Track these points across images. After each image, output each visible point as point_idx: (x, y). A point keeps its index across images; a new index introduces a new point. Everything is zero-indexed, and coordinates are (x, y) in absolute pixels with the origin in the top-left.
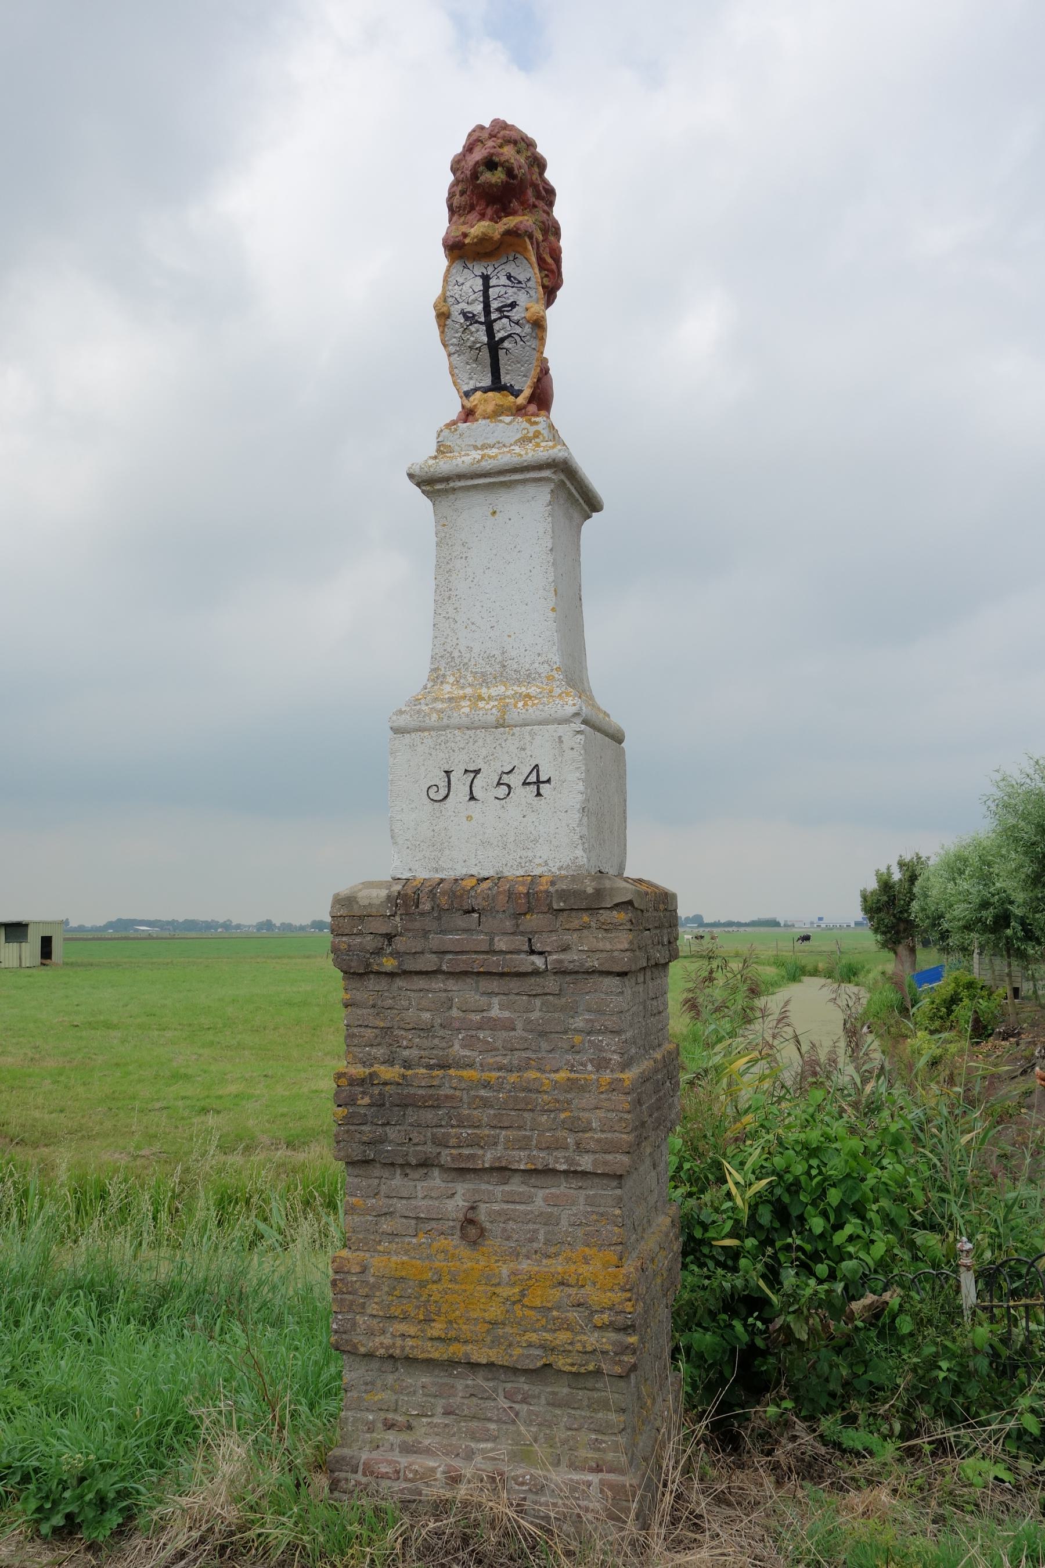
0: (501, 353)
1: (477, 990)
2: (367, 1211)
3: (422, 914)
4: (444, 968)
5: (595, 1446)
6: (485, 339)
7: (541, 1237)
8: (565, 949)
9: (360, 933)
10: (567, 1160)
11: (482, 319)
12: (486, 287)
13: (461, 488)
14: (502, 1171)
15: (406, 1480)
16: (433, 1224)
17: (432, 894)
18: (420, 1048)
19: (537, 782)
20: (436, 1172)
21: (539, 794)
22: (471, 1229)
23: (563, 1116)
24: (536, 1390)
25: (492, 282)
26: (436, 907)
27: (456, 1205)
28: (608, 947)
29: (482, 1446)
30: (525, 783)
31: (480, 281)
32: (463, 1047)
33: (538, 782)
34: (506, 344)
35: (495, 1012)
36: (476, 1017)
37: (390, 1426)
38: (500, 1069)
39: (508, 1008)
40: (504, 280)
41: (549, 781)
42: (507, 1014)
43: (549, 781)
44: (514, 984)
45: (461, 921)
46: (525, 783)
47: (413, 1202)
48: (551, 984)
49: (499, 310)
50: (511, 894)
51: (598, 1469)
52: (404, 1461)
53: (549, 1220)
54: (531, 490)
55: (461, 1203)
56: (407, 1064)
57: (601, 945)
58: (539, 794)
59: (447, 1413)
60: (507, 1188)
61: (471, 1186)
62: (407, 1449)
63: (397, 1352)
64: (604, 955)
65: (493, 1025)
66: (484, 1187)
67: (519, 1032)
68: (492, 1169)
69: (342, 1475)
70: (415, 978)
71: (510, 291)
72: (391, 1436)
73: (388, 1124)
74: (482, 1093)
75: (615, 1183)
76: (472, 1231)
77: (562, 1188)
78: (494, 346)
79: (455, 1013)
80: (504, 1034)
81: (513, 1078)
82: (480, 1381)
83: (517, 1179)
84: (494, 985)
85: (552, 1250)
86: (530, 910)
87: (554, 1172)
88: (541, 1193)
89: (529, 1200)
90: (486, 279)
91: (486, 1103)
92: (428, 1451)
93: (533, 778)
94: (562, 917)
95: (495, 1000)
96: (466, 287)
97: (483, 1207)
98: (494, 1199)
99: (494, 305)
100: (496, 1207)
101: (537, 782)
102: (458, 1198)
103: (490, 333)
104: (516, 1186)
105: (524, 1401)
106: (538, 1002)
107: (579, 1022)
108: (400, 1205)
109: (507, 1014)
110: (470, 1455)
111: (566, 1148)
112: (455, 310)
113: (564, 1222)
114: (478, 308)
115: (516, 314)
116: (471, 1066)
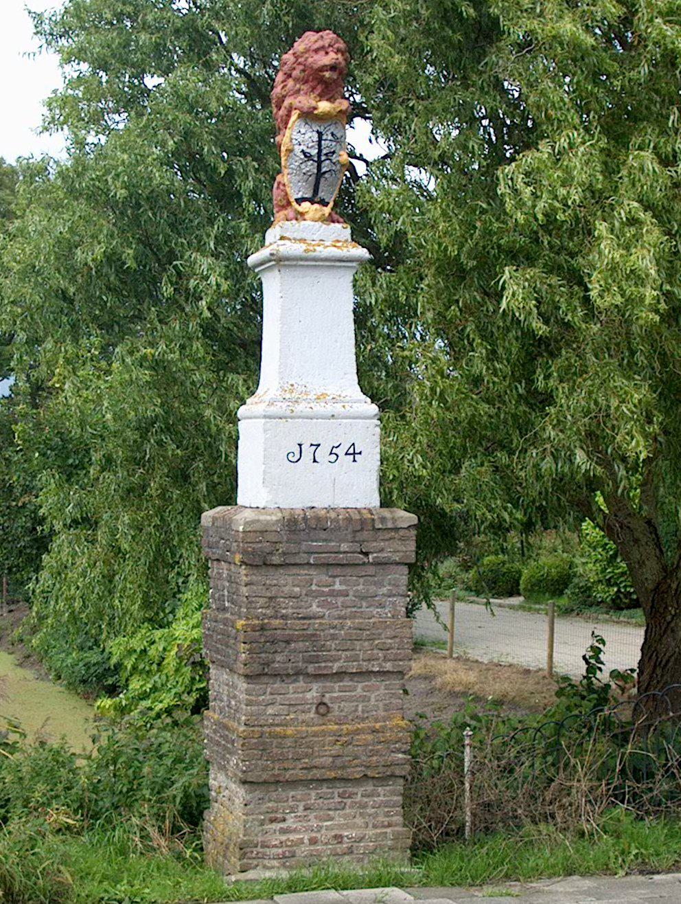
0: (322, 180)
1: (327, 575)
2: (258, 704)
3: (300, 531)
4: (312, 561)
5: (387, 815)
6: (315, 171)
7: (360, 709)
8: (382, 550)
9: (260, 542)
10: (380, 666)
11: (316, 159)
12: (320, 140)
13: (302, 266)
14: (340, 675)
15: (287, 846)
16: (300, 707)
17: (305, 519)
18: (293, 608)
19: (353, 453)
20: (301, 678)
21: (354, 461)
22: (322, 707)
23: (377, 642)
24: (355, 790)
25: (324, 137)
26: (308, 527)
27: (313, 694)
28: (404, 549)
29: (325, 824)
30: (346, 454)
31: (316, 135)
32: (318, 607)
33: (354, 453)
34: (326, 175)
35: (337, 587)
36: (326, 589)
37: (272, 821)
38: (339, 618)
39: (345, 584)
40: (330, 137)
41: (360, 453)
42: (344, 587)
43: (360, 453)
44: (349, 570)
45: (323, 535)
46: (346, 454)
47: (288, 696)
48: (371, 570)
49: (326, 154)
50: (349, 520)
51: (389, 825)
52: (283, 838)
53: (365, 699)
54: (342, 272)
55: (315, 694)
56: (284, 617)
57: (400, 548)
58: (354, 461)
59: (306, 809)
60: (341, 684)
61: (320, 684)
62: (284, 831)
63: (281, 779)
64: (402, 554)
65: (333, 594)
66: (328, 684)
67: (351, 597)
68: (336, 673)
69: (248, 850)
70: (291, 567)
71: (334, 144)
72: (274, 826)
73: (276, 652)
74: (332, 631)
75: (400, 677)
76: (322, 710)
77: (373, 681)
78: (320, 174)
79: (314, 588)
80: (342, 599)
81: (349, 623)
82: (325, 790)
83: (347, 678)
84: (338, 571)
85: (366, 715)
86: (362, 529)
87: (372, 672)
88: (360, 685)
89: (354, 689)
90: (320, 134)
91: (333, 637)
92: (295, 831)
93: (351, 451)
94: (380, 533)
95: (337, 580)
96: (307, 137)
97: (327, 695)
98: (335, 691)
99: (324, 152)
100: (335, 695)
101: (353, 453)
102: (313, 693)
103: (319, 168)
104: (347, 683)
105: (349, 797)
106: (361, 580)
107: (384, 590)
108: (278, 698)
109: (344, 587)
110: (320, 828)
111: (377, 659)
112: (298, 149)
113: (373, 699)
114: (314, 152)
115: (334, 158)
116: (322, 617)
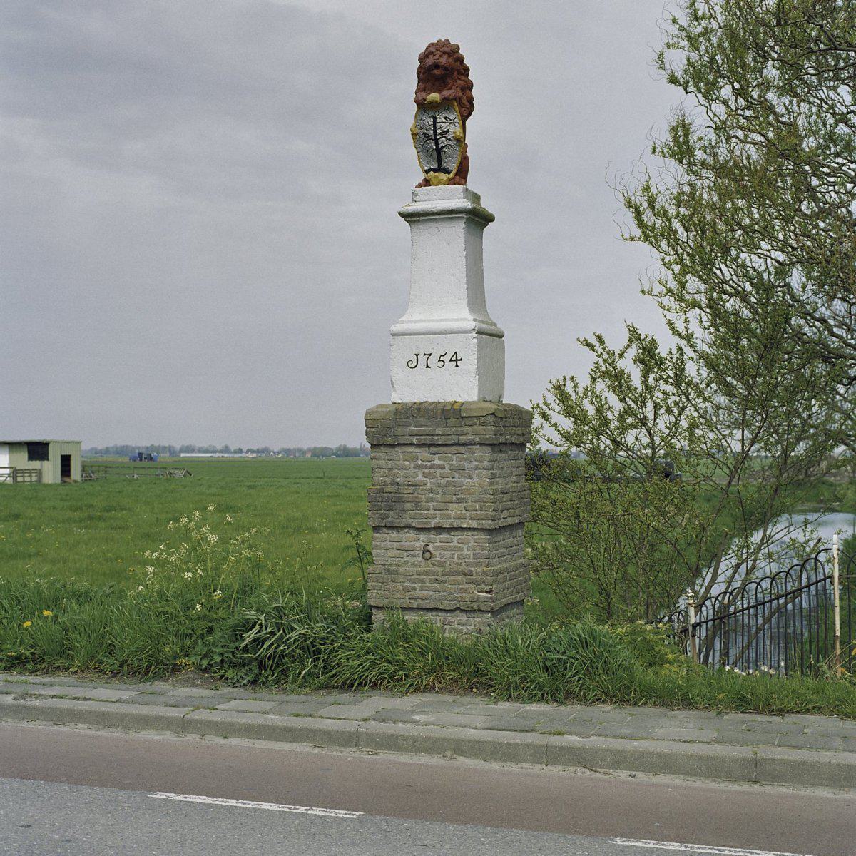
7: (456, 556)
12: (435, 123)
18: (404, 477)
19: (456, 360)
21: (457, 366)
25: (438, 120)
30: (451, 360)
33: (457, 360)
34: (445, 149)
35: (437, 462)
36: (428, 464)
40: (444, 120)
41: (461, 360)
42: (441, 462)
43: (461, 360)
46: (451, 360)
49: (440, 134)
50: (443, 411)
54: (456, 222)
58: (457, 366)
66: (432, 536)
76: (427, 555)
77: (465, 535)
87: (461, 528)
93: (454, 358)
95: (436, 456)
98: (437, 540)
99: (439, 131)
101: (456, 360)
103: (437, 144)
104: (444, 536)
105: (449, 624)
106: (454, 457)
115: (450, 135)
